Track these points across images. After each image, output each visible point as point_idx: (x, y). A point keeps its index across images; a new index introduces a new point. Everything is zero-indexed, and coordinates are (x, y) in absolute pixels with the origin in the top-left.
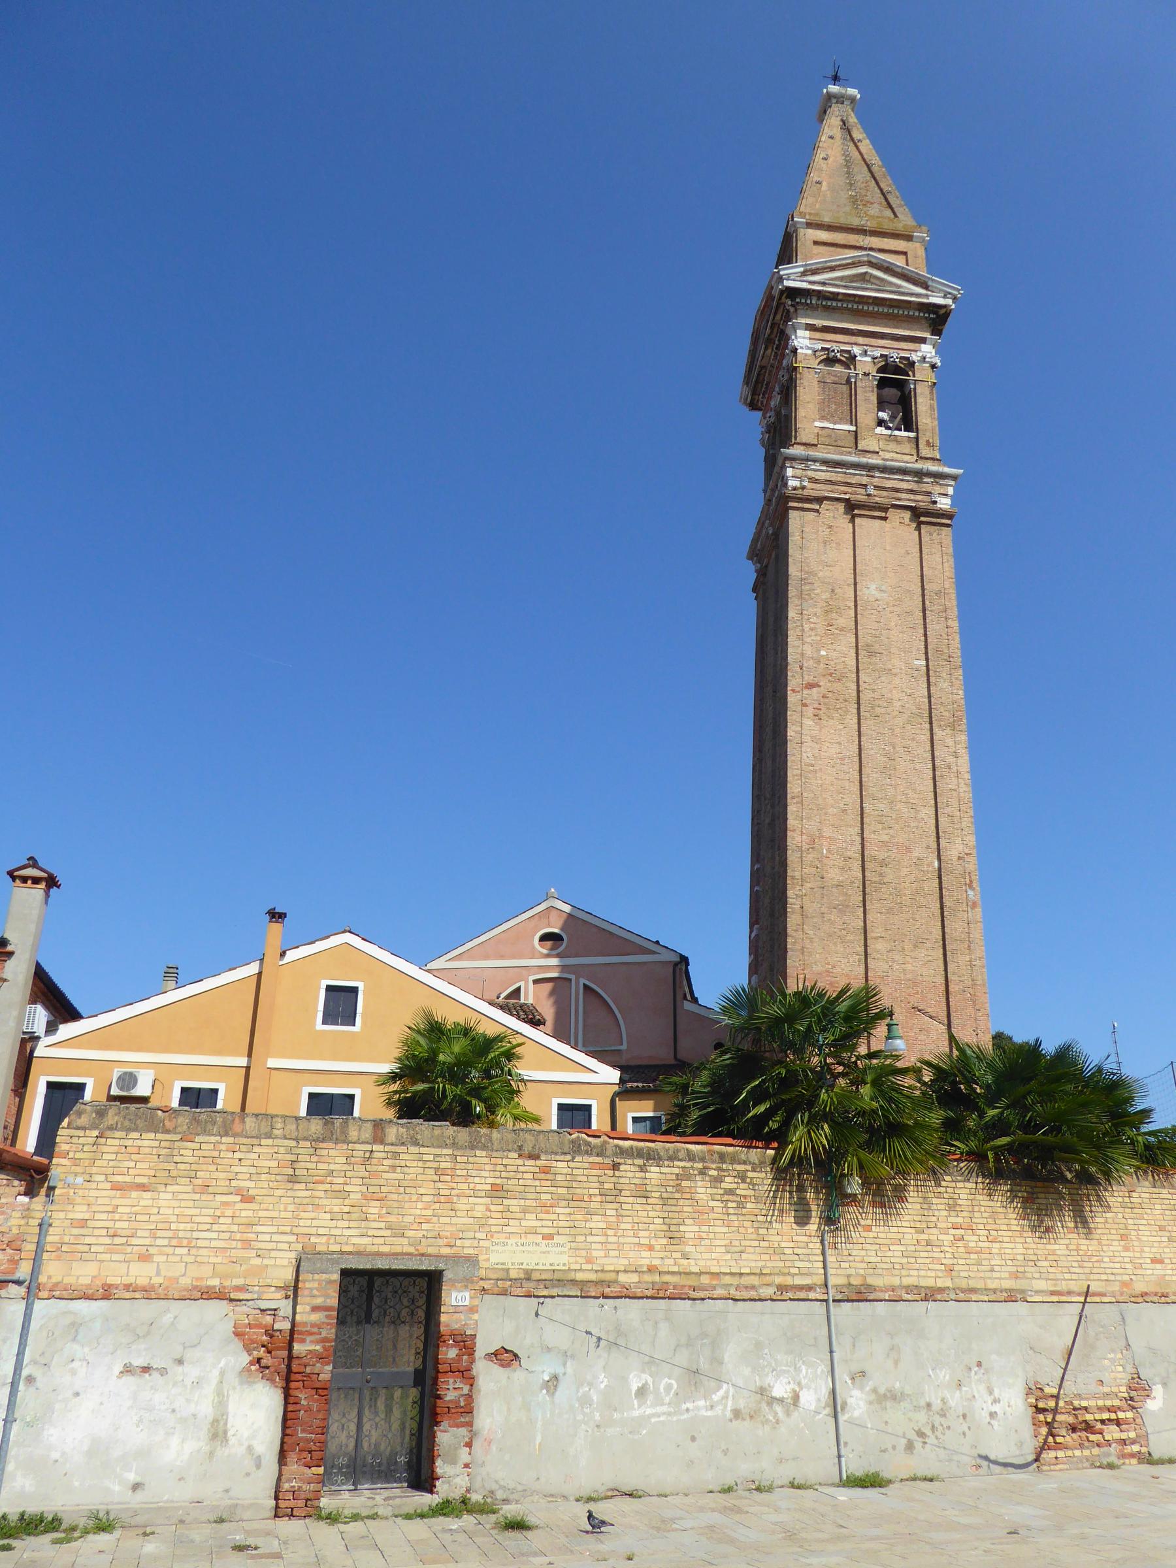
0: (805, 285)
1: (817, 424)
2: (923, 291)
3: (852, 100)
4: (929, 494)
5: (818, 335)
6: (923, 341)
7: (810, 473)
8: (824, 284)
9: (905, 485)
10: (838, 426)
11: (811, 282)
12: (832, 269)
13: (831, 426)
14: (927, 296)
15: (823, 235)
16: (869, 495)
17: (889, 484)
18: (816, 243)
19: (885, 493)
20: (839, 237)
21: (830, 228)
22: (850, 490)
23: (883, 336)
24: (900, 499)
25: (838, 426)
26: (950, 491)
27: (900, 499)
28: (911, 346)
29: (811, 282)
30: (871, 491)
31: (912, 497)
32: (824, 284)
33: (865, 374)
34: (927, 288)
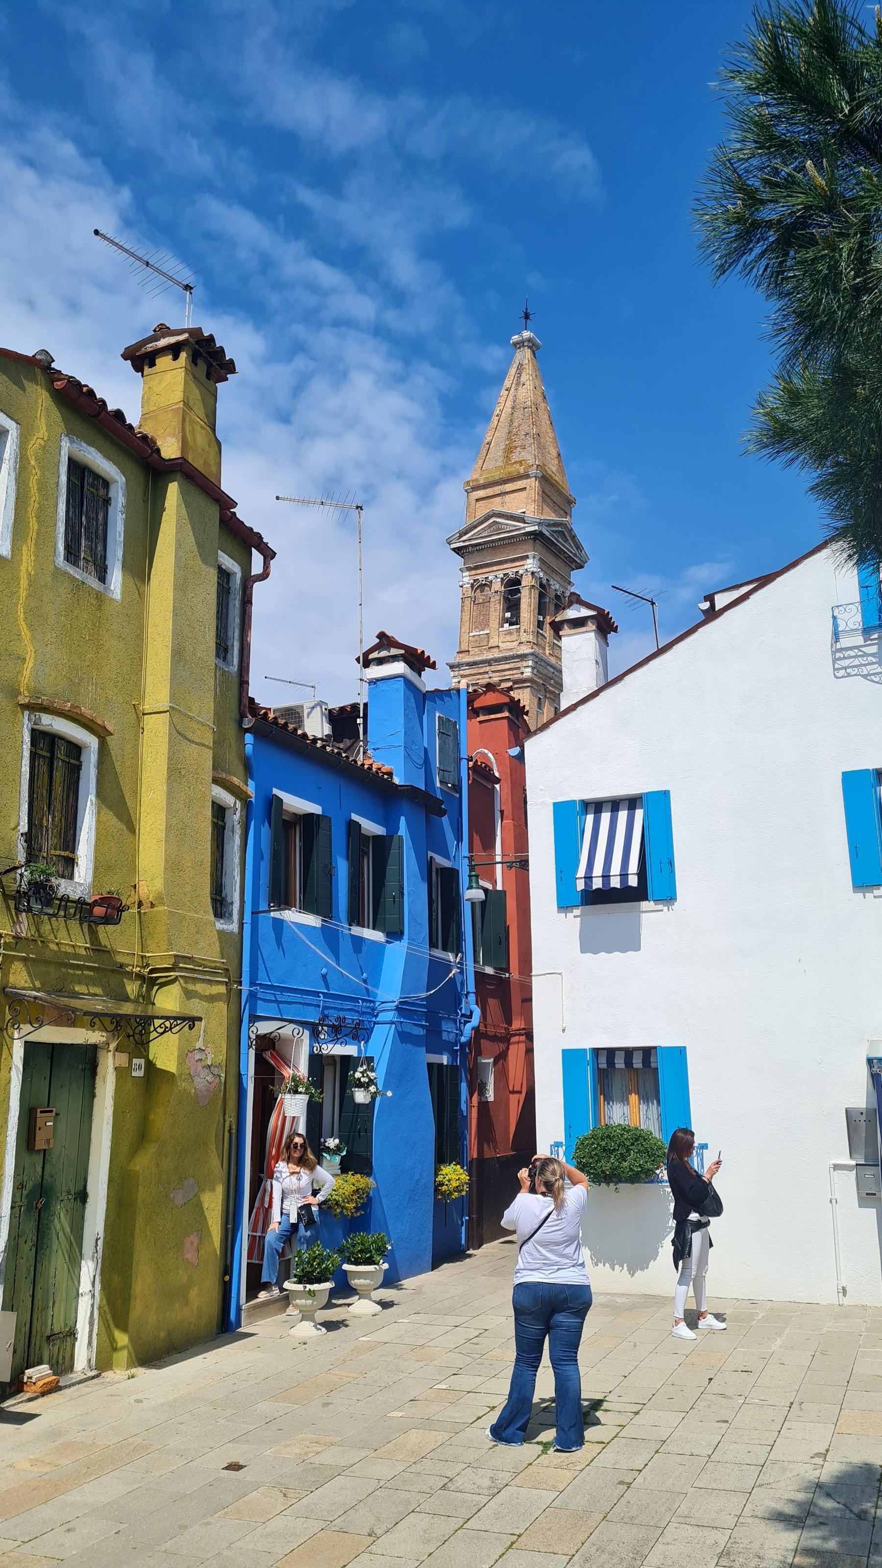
0: (462, 544)
1: (471, 634)
2: (522, 525)
3: (529, 340)
4: (519, 668)
5: (473, 572)
6: (527, 557)
7: (462, 672)
8: (470, 540)
9: (507, 666)
10: (482, 633)
11: (464, 541)
12: (475, 527)
13: (478, 633)
14: (524, 528)
15: (481, 493)
16: (490, 678)
17: (500, 668)
18: (477, 500)
19: (498, 674)
20: (489, 492)
21: (484, 487)
22: (480, 677)
23: (506, 562)
24: (505, 676)
25: (482, 633)
26: (530, 663)
27: (505, 676)
28: (521, 563)
29: (464, 541)
30: (491, 674)
31: (511, 672)
32: (470, 540)
33: (496, 592)
34: (525, 522)
